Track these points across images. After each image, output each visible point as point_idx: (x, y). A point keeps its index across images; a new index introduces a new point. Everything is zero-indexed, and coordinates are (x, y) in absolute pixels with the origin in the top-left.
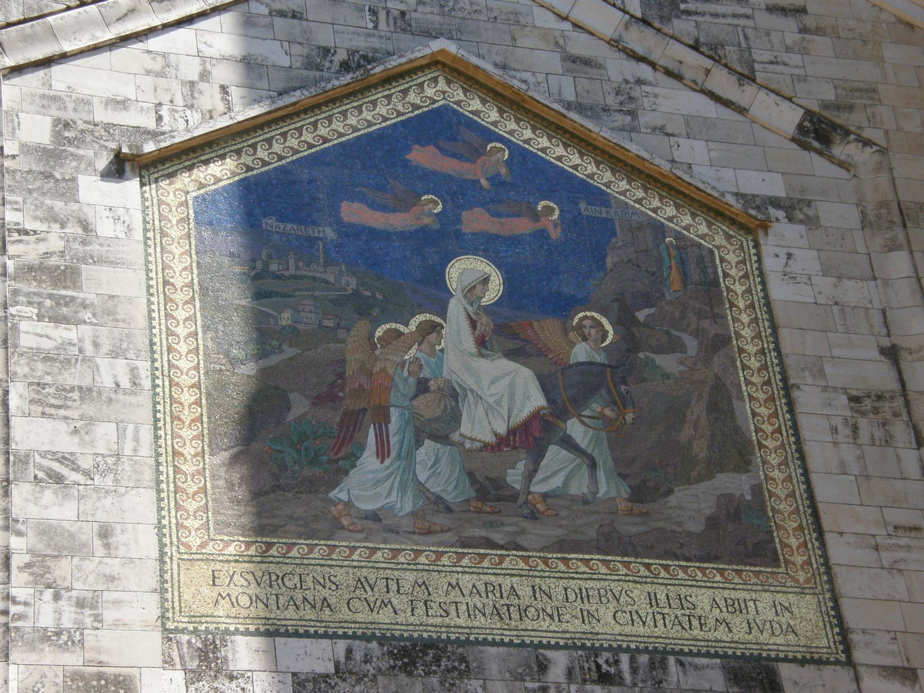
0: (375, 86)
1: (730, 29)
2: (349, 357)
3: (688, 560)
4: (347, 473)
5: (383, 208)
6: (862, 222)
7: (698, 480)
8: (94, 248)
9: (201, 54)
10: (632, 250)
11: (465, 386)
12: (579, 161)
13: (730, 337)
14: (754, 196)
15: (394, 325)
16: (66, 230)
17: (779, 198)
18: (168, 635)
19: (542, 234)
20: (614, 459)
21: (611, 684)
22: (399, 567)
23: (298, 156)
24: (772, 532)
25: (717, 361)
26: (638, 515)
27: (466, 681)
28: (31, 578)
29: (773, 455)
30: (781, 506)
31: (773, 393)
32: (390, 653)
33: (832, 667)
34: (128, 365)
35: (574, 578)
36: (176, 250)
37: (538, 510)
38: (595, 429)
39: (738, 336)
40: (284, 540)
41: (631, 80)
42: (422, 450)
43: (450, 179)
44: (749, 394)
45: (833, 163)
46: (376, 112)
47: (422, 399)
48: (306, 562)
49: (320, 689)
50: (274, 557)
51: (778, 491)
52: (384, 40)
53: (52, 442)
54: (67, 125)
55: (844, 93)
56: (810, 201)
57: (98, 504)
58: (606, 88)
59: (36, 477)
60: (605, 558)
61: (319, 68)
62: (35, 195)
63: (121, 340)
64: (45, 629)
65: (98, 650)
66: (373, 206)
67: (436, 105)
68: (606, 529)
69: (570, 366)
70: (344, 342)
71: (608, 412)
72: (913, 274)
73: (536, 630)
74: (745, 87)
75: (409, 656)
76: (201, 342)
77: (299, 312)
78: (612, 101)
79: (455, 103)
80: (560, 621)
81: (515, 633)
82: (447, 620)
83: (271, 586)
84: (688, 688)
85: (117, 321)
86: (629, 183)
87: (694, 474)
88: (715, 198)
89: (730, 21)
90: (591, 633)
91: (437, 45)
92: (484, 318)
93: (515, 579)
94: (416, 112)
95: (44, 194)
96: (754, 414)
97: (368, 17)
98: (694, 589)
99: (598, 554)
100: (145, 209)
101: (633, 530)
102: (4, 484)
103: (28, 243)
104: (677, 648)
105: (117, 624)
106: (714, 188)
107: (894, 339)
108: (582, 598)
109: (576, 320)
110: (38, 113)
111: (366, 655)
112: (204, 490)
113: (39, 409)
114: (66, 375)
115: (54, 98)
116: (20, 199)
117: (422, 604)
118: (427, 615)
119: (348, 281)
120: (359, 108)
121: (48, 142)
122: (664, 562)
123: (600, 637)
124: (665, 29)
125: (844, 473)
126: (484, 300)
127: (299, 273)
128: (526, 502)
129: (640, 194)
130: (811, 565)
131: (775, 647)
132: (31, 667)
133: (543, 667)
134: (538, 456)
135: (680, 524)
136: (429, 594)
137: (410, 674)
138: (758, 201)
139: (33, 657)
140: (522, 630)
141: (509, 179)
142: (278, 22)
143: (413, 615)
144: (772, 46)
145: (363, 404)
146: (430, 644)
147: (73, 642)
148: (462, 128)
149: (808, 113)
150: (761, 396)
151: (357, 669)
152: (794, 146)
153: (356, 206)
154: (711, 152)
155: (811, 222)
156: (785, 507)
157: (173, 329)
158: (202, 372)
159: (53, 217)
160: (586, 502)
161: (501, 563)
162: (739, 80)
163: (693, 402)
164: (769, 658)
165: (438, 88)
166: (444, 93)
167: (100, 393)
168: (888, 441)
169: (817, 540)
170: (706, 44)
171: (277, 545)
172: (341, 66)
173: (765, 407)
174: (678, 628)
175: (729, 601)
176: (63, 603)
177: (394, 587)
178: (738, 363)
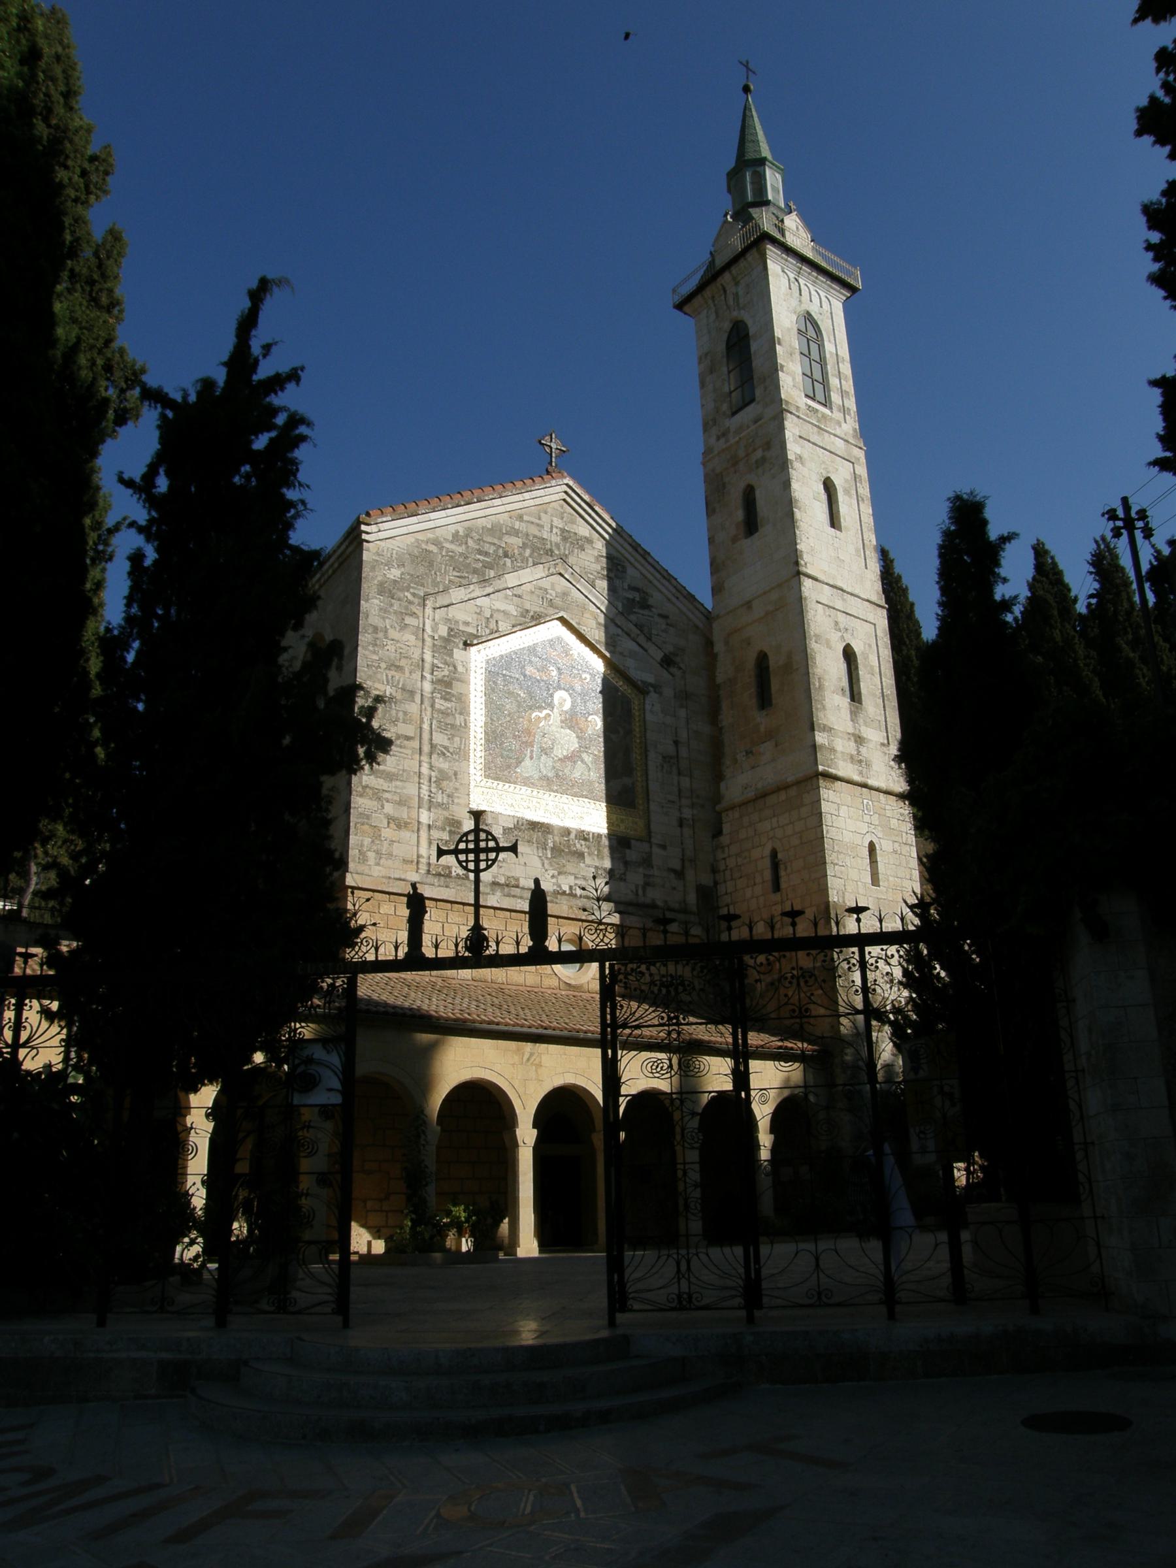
61: (525, 617)
65: (453, 812)
91: (560, 615)
105: (458, 804)
115: (449, 620)
139: (436, 811)
149: (665, 655)
155: (660, 694)
159: (446, 663)
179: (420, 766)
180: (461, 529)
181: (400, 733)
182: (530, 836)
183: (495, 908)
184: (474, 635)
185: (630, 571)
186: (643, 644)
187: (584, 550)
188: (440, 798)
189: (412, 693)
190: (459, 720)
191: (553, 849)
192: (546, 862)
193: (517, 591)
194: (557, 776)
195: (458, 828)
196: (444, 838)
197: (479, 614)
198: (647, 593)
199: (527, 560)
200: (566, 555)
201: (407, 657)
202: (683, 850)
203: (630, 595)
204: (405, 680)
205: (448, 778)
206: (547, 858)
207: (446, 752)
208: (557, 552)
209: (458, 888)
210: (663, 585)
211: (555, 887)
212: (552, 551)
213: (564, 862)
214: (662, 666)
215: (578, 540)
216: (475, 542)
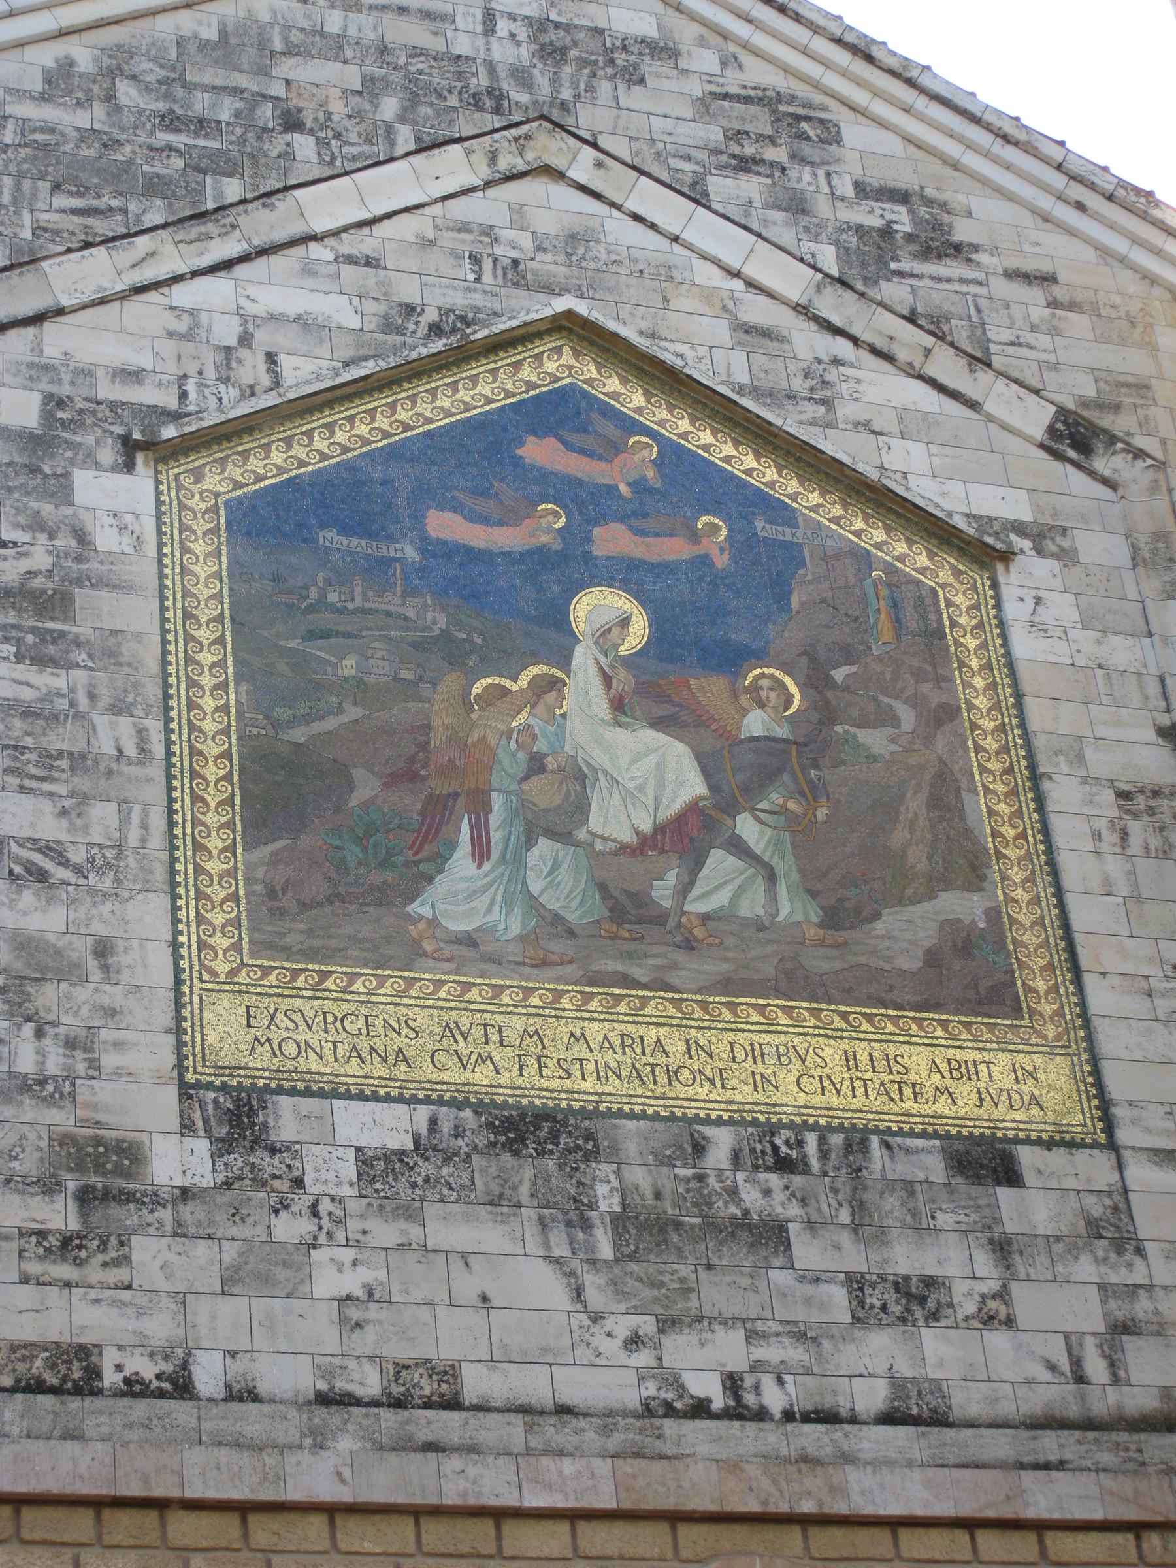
0: (476, 357)
1: (957, 298)
2: (436, 722)
4: (430, 879)
5: (485, 521)
6: (1133, 559)
7: (916, 900)
8: (93, 566)
10: (826, 586)
12: (754, 464)
13: (959, 707)
14: (991, 519)
15: (497, 680)
17: (1023, 522)
18: (186, 1091)
19: (704, 561)
20: (800, 870)
24: (1013, 972)
25: (941, 742)
26: (831, 947)
28: (6, 1007)
29: (1016, 869)
31: (1016, 785)
32: (490, 1126)
33: (1088, 1151)
34: (134, 724)
35: (743, 1031)
36: (201, 571)
38: (774, 828)
39: (970, 706)
40: (344, 969)
41: (826, 359)
42: (534, 853)
43: (580, 483)
44: (984, 786)
45: (1095, 479)
47: (537, 781)
48: (373, 999)
51: (1021, 917)
52: (489, 297)
54: (61, 404)
56: (1065, 529)
57: (94, 912)
58: (792, 367)
59: (11, 872)
61: (400, 331)
62: (16, 495)
63: (125, 691)
64: (25, 1076)
65: (95, 1107)
66: (471, 517)
68: (789, 965)
69: (742, 741)
71: (792, 805)
74: (977, 375)
75: (516, 1130)
76: (232, 697)
77: (367, 658)
78: (799, 385)
79: (584, 382)
80: (723, 1087)
81: (662, 1102)
82: (568, 1084)
83: (326, 1031)
85: (121, 665)
86: (822, 495)
87: (909, 892)
88: (940, 519)
89: (956, 286)
90: (766, 1104)
91: (561, 304)
92: (622, 674)
93: (662, 1030)
94: (532, 393)
95: (28, 494)
96: (991, 812)
97: (468, 266)
98: (907, 1047)
100: (159, 515)
101: (825, 966)
103: (5, 559)
104: (883, 1126)
105: (118, 1073)
106: (937, 506)
108: (754, 1057)
109: (750, 678)
110: (24, 388)
111: (456, 1127)
112: (235, 897)
113: (17, 781)
114: (52, 736)
115: (46, 368)
117: (533, 1060)
118: (541, 1076)
120: (454, 386)
121: (35, 425)
122: (867, 1011)
123: (778, 1109)
124: (872, 292)
127: (367, 605)
128: (679, 925)
129: (838, 511)
130: (1063, 1015)
131: (1013, 1125)
132: (8, 1125)
133: (699, 1148)
134: (699, 864)
135: (890, 959)
136: (544, 1048)
137: (516, 1154)
138: (997, 526)
141: (658, 485)
142: (347, 270)
144: (1013, 323)
145: (454, 787)
146: (543, 1116)
147: (62, 1094)
148: (594, 416)
149: (1062, 412)
150: (1001, 788)
151: (443, 1146)
152: (1042, 454)
153: (448, 515)
155: (1067, 557)
156: (1030, 938)
158: (234, 738)
159: (38, 525)
160: (761, 928)
161: (642, 1007)
162: (970, 364)
164: (1005, 1139)
166: (570, 368)
170: (925, 316)
172: (430, 330)
174: (884, 1098)
176: (47, 1042)
178: (970, 743)
180: (83, 53)
182: (503, 1178)
183: (331, 1511)
185: (855, 134)
187: (642, 81)
191: (619, 1223)
192: (593, 1283)
193: (351, 244)
194: (618, 914)
196: (56, 1223)
198: (943, 206)
199: (389, 131)
200: (564, 106)
203: (870, 216)
205: (72, 973)
206: (594, 1263)
207: (49, 865)
208: (523, 98)
209: (134, 1435)
210: (1008, 167)
211: (650, 1389)
212: (498, 100)
213: (685, 1271)
215: (609, 52)
216: (148, 89)
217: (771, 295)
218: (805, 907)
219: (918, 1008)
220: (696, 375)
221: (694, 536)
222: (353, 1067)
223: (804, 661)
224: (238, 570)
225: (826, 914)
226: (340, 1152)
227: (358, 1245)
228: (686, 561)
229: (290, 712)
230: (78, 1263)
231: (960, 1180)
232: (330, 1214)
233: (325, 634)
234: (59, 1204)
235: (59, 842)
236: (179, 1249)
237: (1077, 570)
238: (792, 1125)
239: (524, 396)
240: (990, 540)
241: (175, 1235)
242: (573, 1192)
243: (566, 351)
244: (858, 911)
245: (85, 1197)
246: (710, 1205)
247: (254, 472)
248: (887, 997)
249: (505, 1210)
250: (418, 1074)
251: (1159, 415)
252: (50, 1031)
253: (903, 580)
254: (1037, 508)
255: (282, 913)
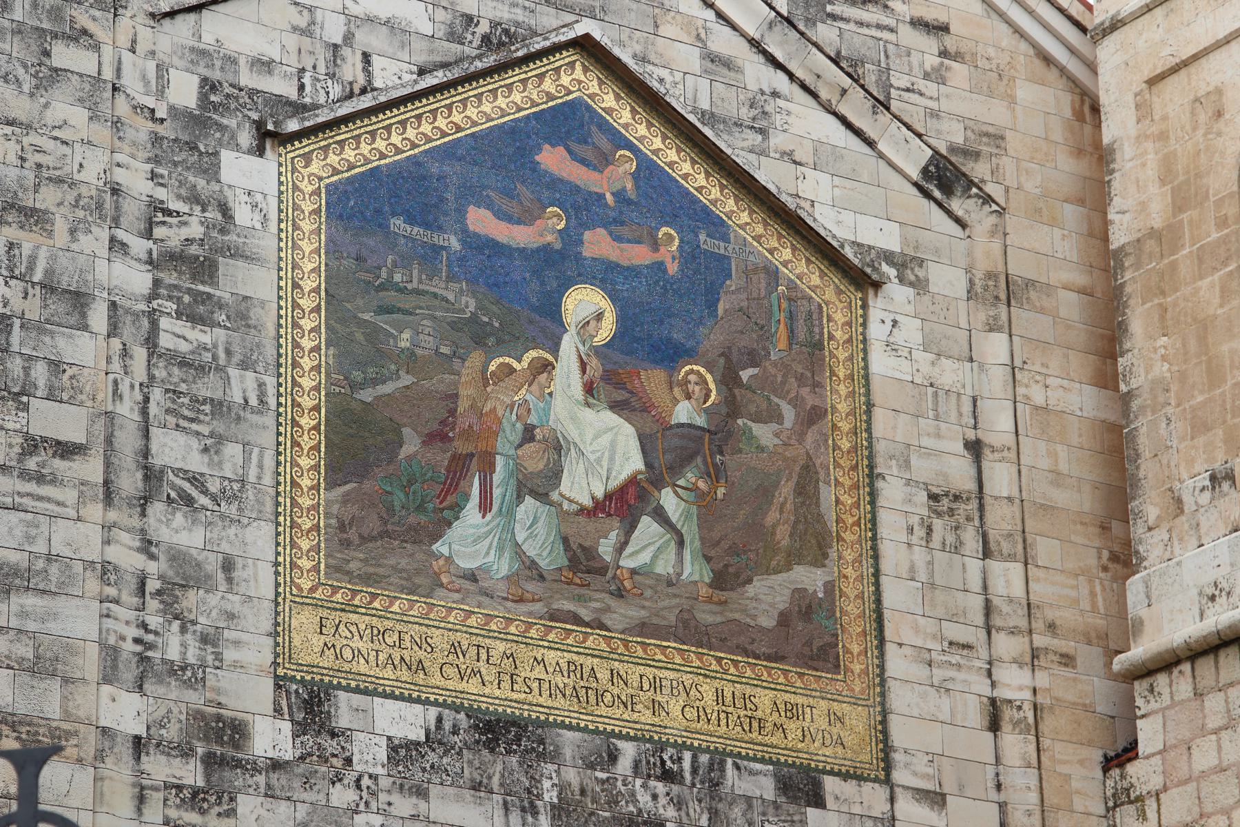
1: (871, 42)
2: (463, 392)
3: (757, 657)
4: (450, 524)
5: (509, 218)
7: (777, 571)
9: (346, 12)
11: (570, 439)
12: (704, 183)
13: (826, 410)
15: (507, 360)
16: (206, 214)
18: (279, 683)
19: (660, 266)
20: (702, 539)
21: (673, 783)
22: (491, 634)
23: (431, 145)
24: (837, 635)
25: (810, 438)
26: (716, 603)
27: (542, 764)
28: (162, 607)
29: (849, 550)
30: (849, 608)
31: (858, 480)
33: (871, 784)
35: (650, 666)
36: (307, 247)
37: (624, 587)
40: (387, 593)
41: (767, 91)
42: (522, 507)
43: (576, 189)
44: (836, 479)
46: (510, 99)
47: (529, 448)
48: (405, 618)
49: (411, 756)
50: (377, 610)
52: (527, 13)
53: (184, 458)
55: (973, 137)
57: (224, 534)
58: (742, 97)
59: (168, 495)
60: (681, 647)
63: (251, 350)
65: (218, 691)
67: (571, 97)
68: (686, 616)
69: (671, 427)
70: (459, 374)
71: (701, 484)
72: (1010, 363)
73: (610, 718)
75: (493, 732)
76: (323, 359)
77: (418, 333)
78: (745, 114)
80: (632, 710)
84: (741, 793)
87: (774, 563)
89: (874, 32)
90: (660, 726)
91: (580, 29)
93: (596, 661)
94: (550, 104)
95: (188, 169)
96: (838, 501)
98: (759, 689)
99: (675, 642)
101: (710, 619)
102: (142, 502)
105: (237, 666)
106: (834, 237)
107: (980, 434)
108: (655, 688)
109: (682, 374)
110: (187, 71)
111: (454, 726)
115: (203, 53)
116: (166, 173)
117: (508, 677)
118: (512, 690)
119: (467, 302)
121: (194, 107)
123: (667, 731)
125: (913, 579)
126: (596, 339)
127: (421, 287)
129: (759, 229)
131: (823, 759)
133: (613, 757)
134: (633, 527)
135: (754, 617)
136: (516, 668)
137: (492, 751)
139: (161, 690)
140: (597, 716)
141: (633, 197)
143: (499, 688)
144: (911, 70)
145: (470, 448)
146: (514, 722)
147: (196, 679)
150: (848, 483)
152: (915, 191)
153: (484, 213)
154: (835, 189)
155: (920, 285)
156: (852, 608)
157: (298, 340)
158: (323, 393)
159: (194, 198)
160: (670, 584)
162: (874, 107)
163: (783, 483)
164: (816, 769)
165: (573, 76)
166: (580, 82)
167: (229, 408)
168: (957, 548)
169: (877, 648)
171: (381, 597)
173: (849, 495)
175: (788, 705)
176: (189, 636)
177: (484, 656)
178: (830, 442)
179: (107, 542)
181: (36, 430)
184: (289, 103)
186: (857, 123)
188: (173, 647)
189: (79, 300)
190: (241, 385)
194: (574, 564)
195: (237, 747)
196: (189, 781)
197: (306, 32)
201: (59, 181)
202: (1002, 806)
204: (53, 258)
207: (194, 493)
214: (927, 194)
217: (734, 27)
218: (701, 569)
219: (769, 658)
220: (674, 104)
221: (655, 246)
222: (388, 673)
223: (722, 360)
224: (333, 249)
225: (715, 577)
226: (377, 739)
227: (385, 814)
228: (647, 266)
229: (362, 376)
230: (203, 812)
231: (784, 799)
232: (368, 788)
233: (388, 310)
234: (191, 766)
235: (202, 475)
236: (269, 806)
237: (926, 298)
238: (675, 745)
239: (544, 106)
240: (868, 270)
241: (266, 795)
242: (527, 785)
243: (578, 66)
244: (737, 575)
245: (210, 762)
246: (616, 803)
247: (348, 160)
248: (750, 647)
249: (482, 794)
250: (432, 682)
251: (1007, 163)
252: (191, 628)
253: (800, 295)
254: (905, 240)
255: (346, 544)
